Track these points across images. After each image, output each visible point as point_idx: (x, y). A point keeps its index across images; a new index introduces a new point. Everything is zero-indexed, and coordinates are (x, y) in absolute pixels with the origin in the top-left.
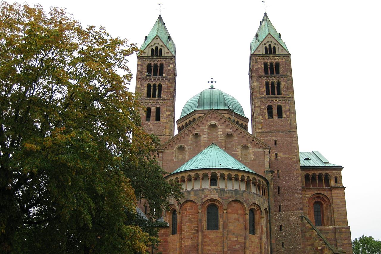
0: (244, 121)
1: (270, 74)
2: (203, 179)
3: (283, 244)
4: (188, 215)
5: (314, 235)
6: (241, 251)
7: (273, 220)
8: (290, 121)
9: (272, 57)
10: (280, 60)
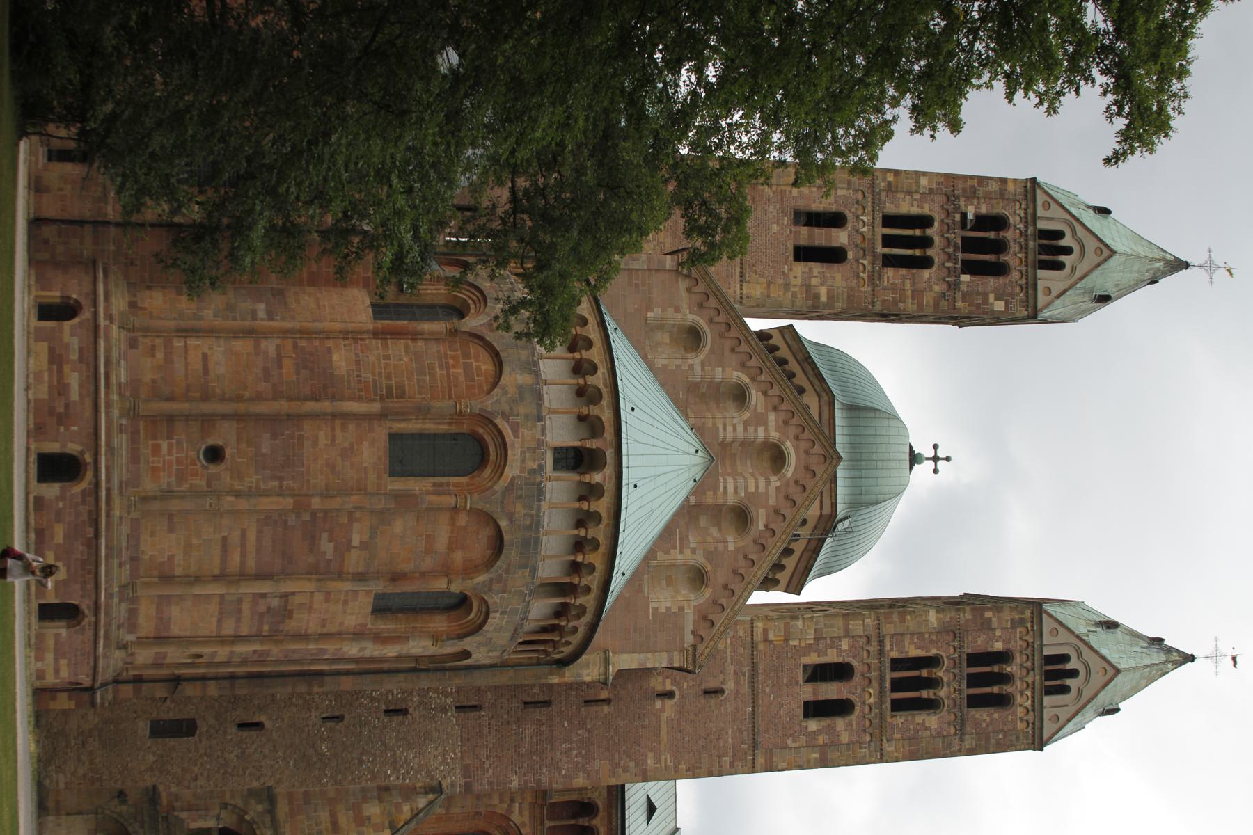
0: (791, 578)
1: (969, 675)
2: (581, 418)
3: (337, 718)
4: (447, 363)
7: (424, 682)
8: (794, 745)
9: (1030, 680)
10: (1020, 712)
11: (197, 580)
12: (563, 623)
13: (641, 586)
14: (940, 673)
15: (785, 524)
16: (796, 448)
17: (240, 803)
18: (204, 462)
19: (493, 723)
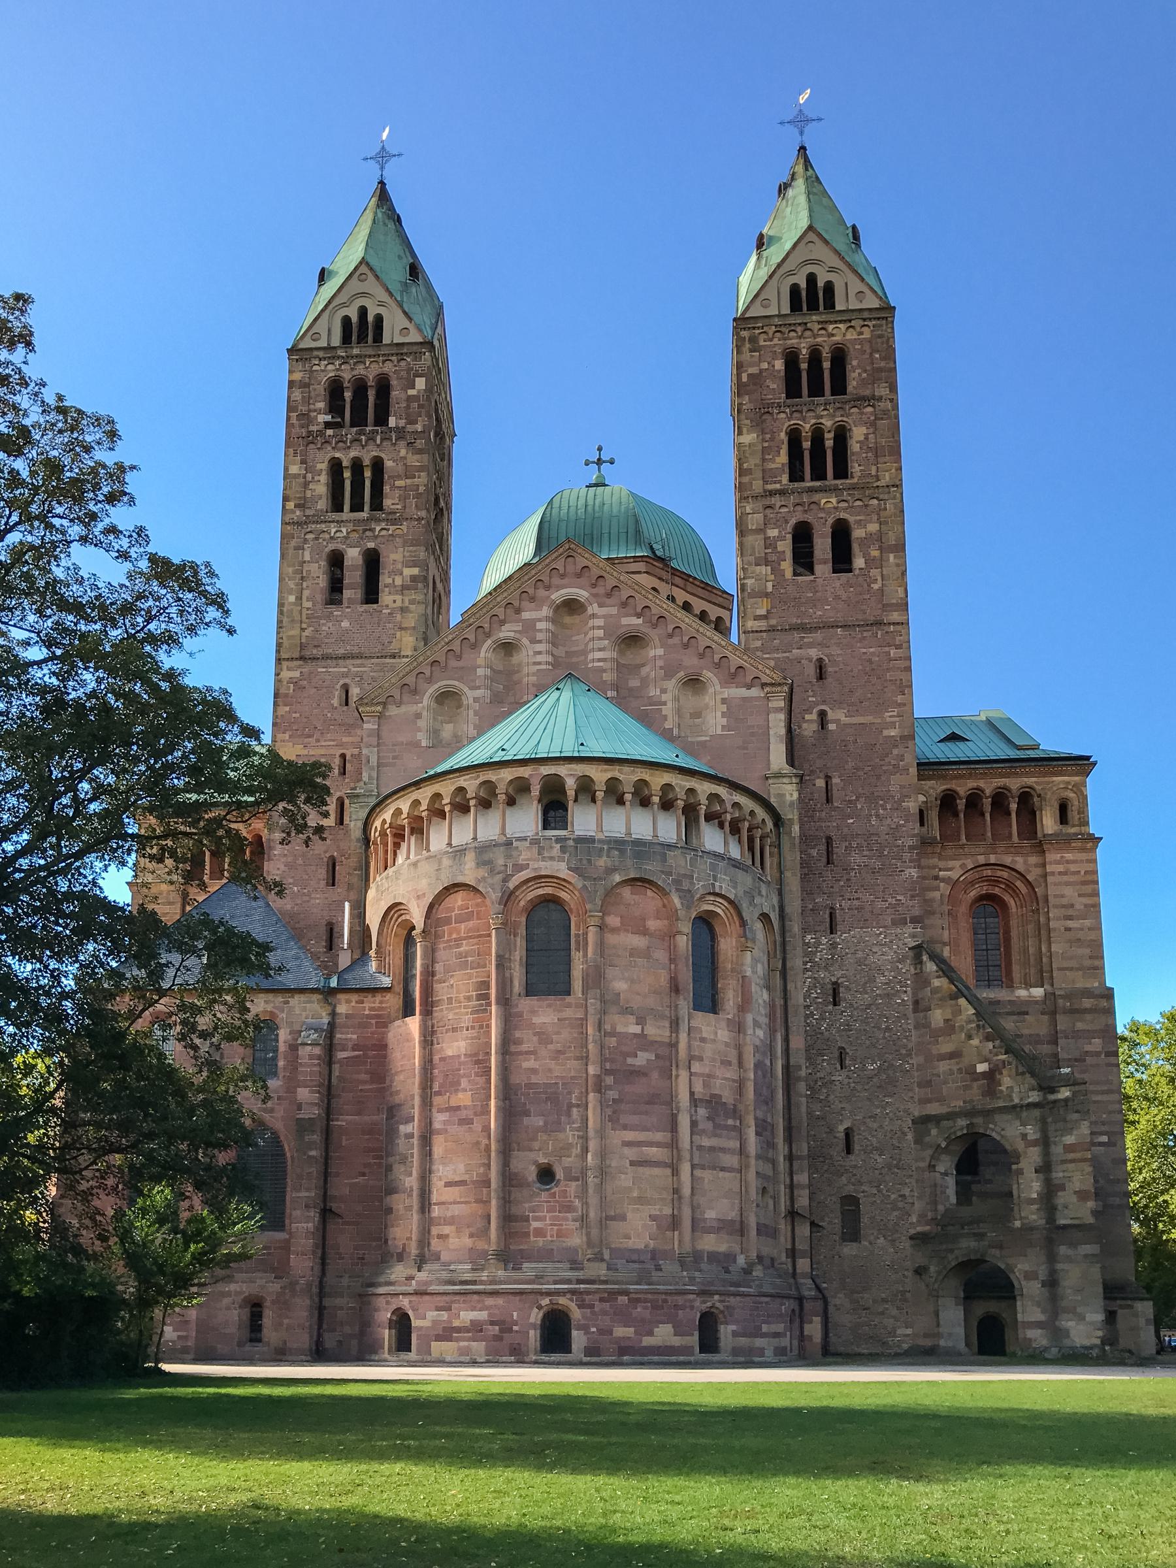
4: (456, 940)
6: (655, 1075)
7: (796, 962)
10: (851, 335)
11: (676, 1191)
13: (699, 743)
14: (807, 427)
15: (637, 596)
16: (559, 588)
19: (848, 896)
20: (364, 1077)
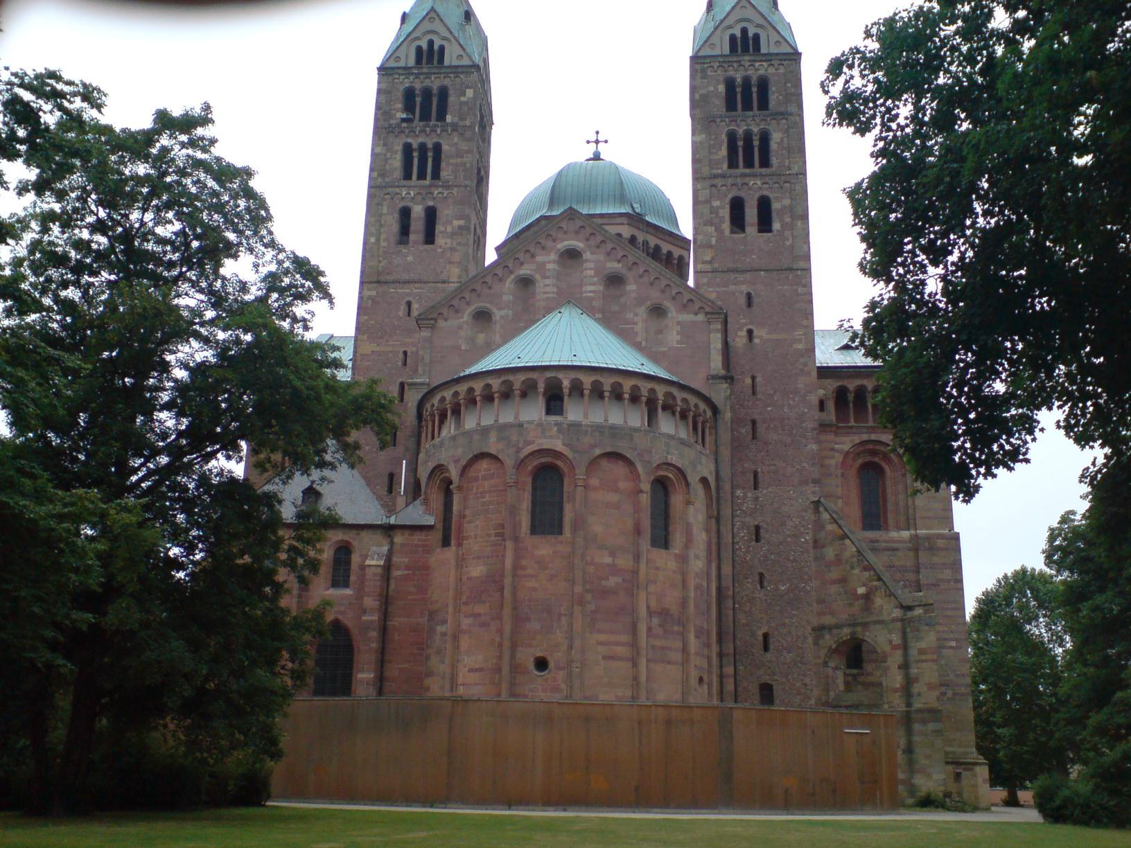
0: (677, 246)
2: (524, 395)
5: (847, 554)
8: (791, 240)
9: (747, 64)
10: (771, 70)
11: (635, 678)
12: (679, 409)
14: (741, 131)
15: (618, 248)
17: (823, 653)
18: (546, 672)
20: (412, 589)
